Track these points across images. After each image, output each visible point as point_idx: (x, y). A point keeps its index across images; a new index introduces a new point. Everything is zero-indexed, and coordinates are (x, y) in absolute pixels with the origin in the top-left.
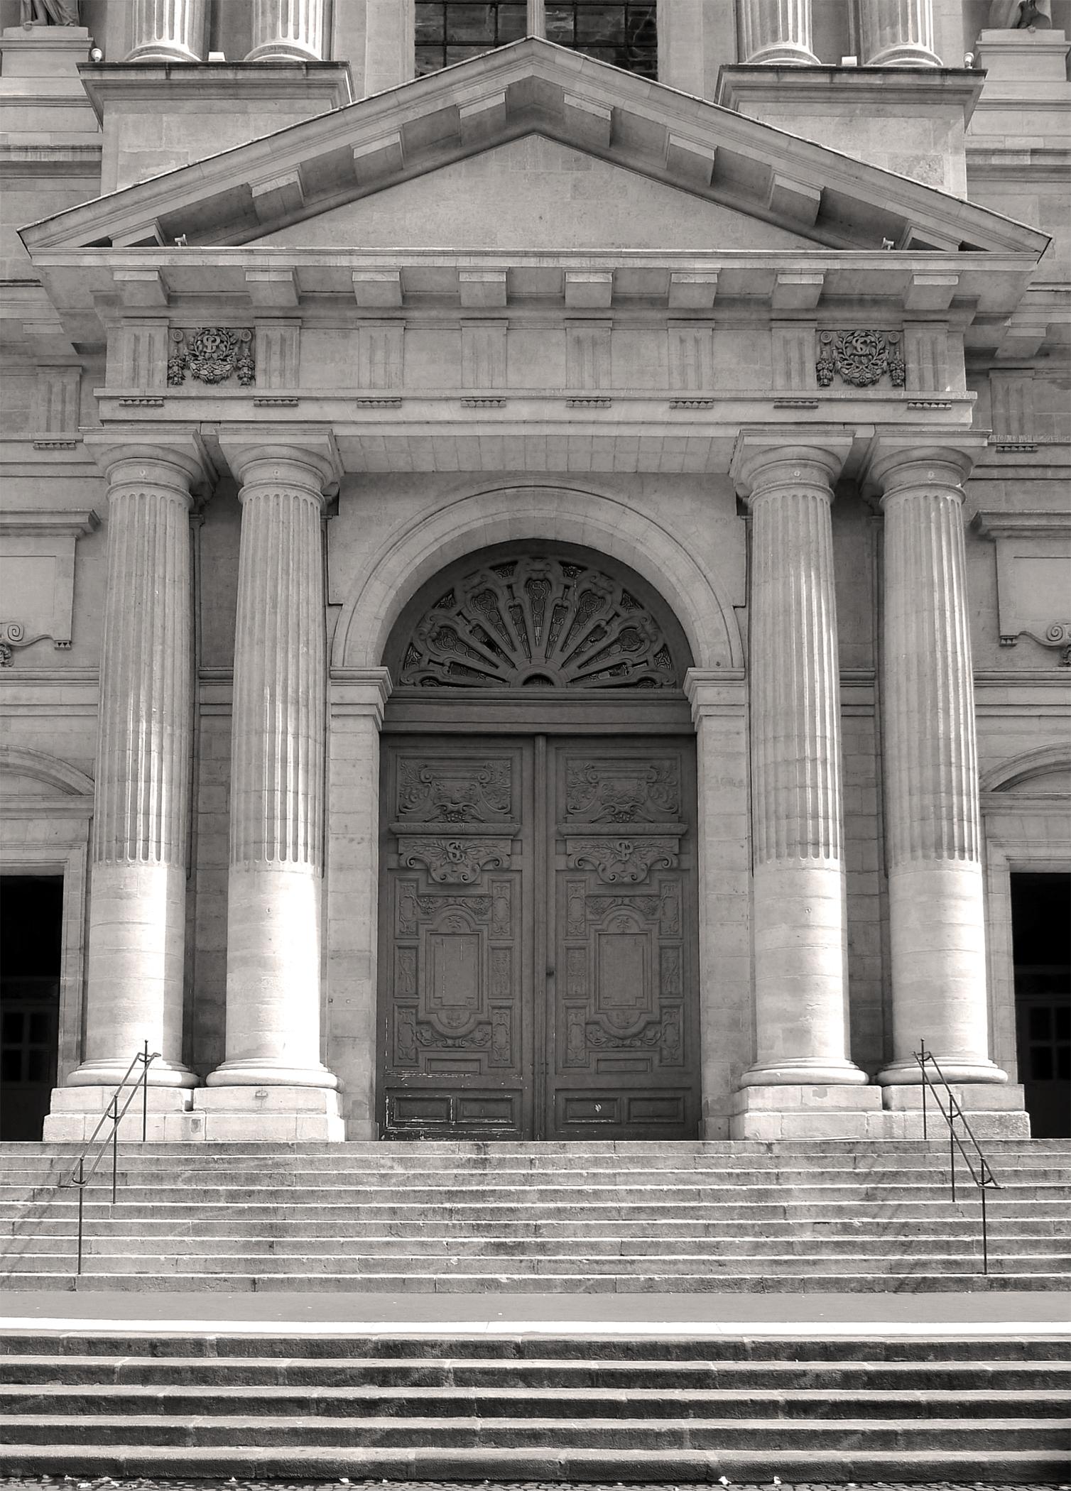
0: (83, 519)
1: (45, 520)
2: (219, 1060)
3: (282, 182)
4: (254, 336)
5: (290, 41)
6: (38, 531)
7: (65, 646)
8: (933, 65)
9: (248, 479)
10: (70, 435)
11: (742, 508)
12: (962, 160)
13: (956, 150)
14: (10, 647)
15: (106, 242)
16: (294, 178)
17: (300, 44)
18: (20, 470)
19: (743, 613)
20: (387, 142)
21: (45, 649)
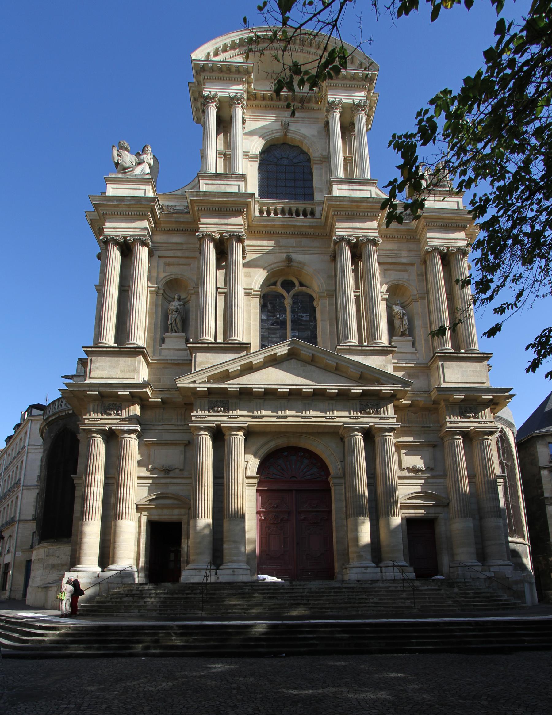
0: (187, 442)
1: (177, 442)
2: (222, 563)
3: (236, 369)
4: (228, 402)
5: (236, 338)
6: (175, 444)
7: (182, 470)
8: (384, 345)
9: (227, 434)
10: (183, 423)
11: (342, 439)
12: (392, 365)
13: (390, 364)
14: (169, 470)
15: (195, 381)
16: (239, 368)
17: (238, 339)
18: (171, 431)
19: (343, 463)
20: (260, 360)
21: (177, 471)
